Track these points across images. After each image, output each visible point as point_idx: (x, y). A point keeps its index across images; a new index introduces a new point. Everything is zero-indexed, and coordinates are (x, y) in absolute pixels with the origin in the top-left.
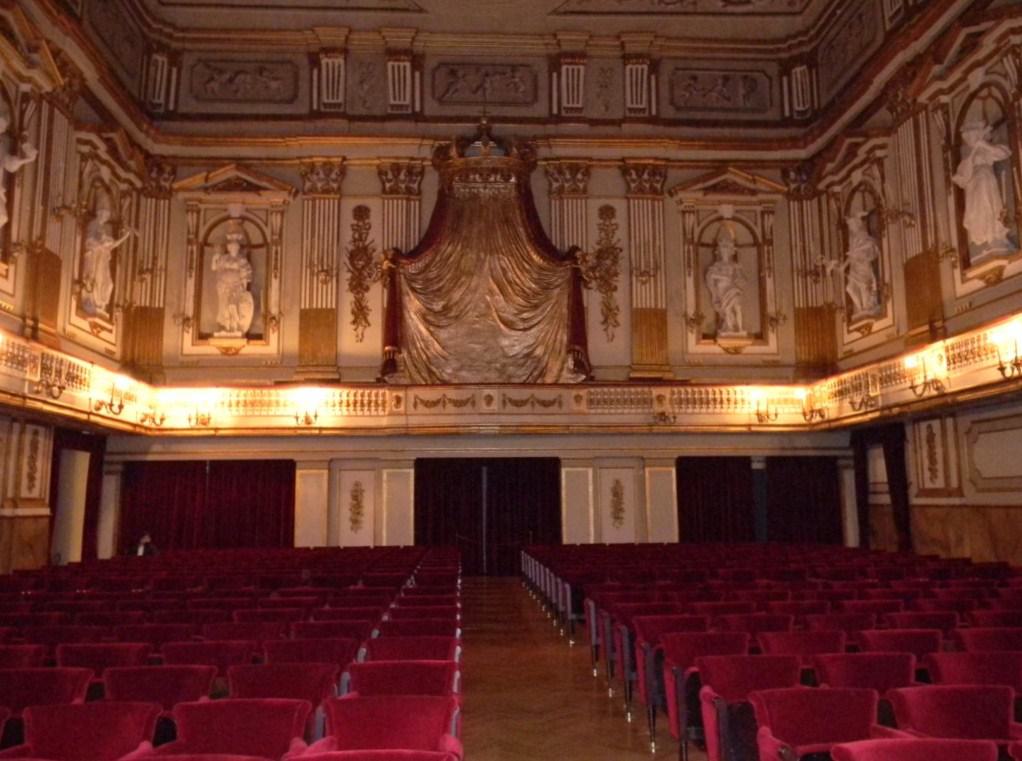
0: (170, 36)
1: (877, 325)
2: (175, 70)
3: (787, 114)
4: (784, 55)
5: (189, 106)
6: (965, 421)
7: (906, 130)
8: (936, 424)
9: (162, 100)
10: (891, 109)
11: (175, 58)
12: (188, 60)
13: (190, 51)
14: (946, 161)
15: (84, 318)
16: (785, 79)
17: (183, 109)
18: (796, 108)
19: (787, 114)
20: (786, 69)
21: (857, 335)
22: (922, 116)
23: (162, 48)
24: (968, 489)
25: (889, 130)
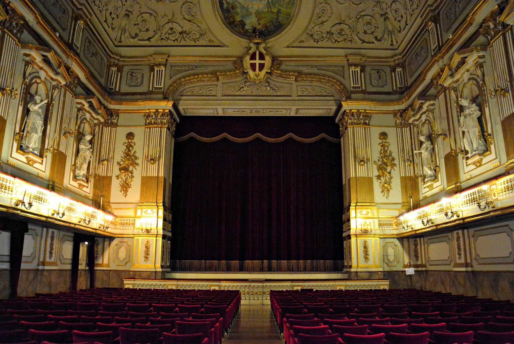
0: (118, 60)
1: (435, 185)
2: (119, 74)
3: (395, 89)
4: (393, 64)
5: (125, 89)
6: (471, 231)
7: (442, 97)
8: (460, 232)
9: (113, 87)
10: (436, 88)
11: (120, 70)
12: (126, 69)
13: (127, 65)
14: (457, 112)
15: (76, 181)
16: (393, 74)
17: (123, 90)
18: (399, 86)
19: (395, 89)
20: (393, 70)
21: (427, 189)
22: (447, 91)
23: (115, 65)
24: (475, 263)
25: (435, 97)
